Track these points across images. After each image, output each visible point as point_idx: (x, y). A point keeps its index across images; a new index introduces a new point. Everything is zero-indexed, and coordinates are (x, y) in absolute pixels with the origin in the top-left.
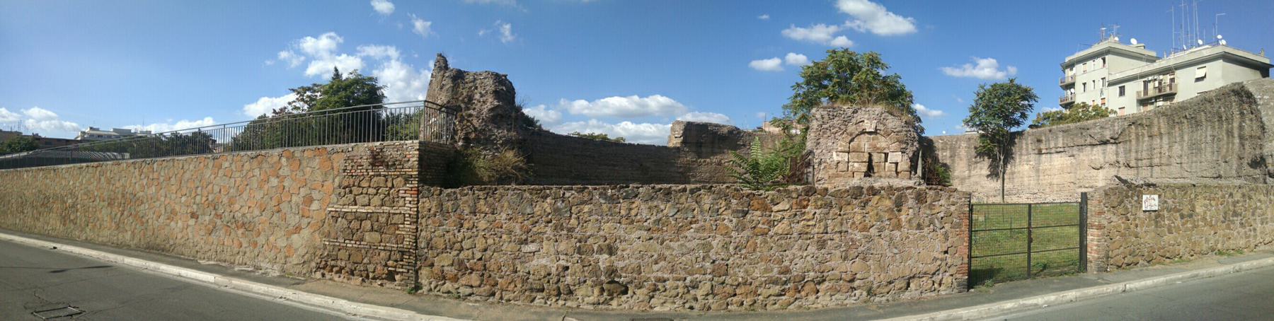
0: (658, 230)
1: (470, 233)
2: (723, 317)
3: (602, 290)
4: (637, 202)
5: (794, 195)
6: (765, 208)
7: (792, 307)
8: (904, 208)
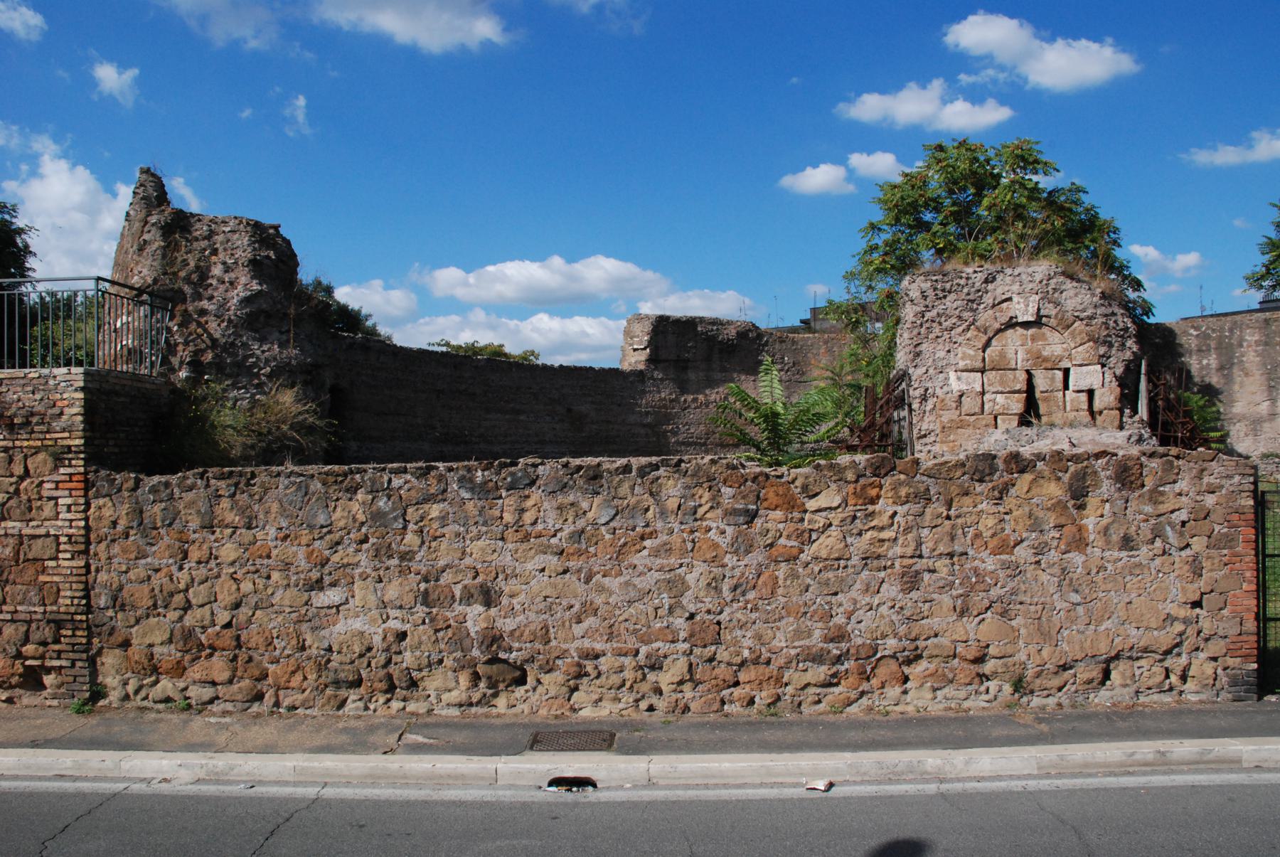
0: (579, 553)
1: (202, 572)
2: (714, 726)
3: (476, 678)
4: (536, 495)
5: (850, 476)
6: (790, 504)
7: (853, 709)
8: (1092, 501)
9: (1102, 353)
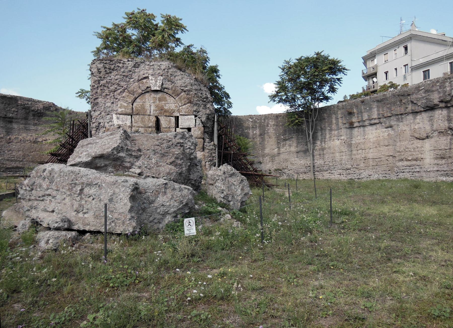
9: (195, 109)
